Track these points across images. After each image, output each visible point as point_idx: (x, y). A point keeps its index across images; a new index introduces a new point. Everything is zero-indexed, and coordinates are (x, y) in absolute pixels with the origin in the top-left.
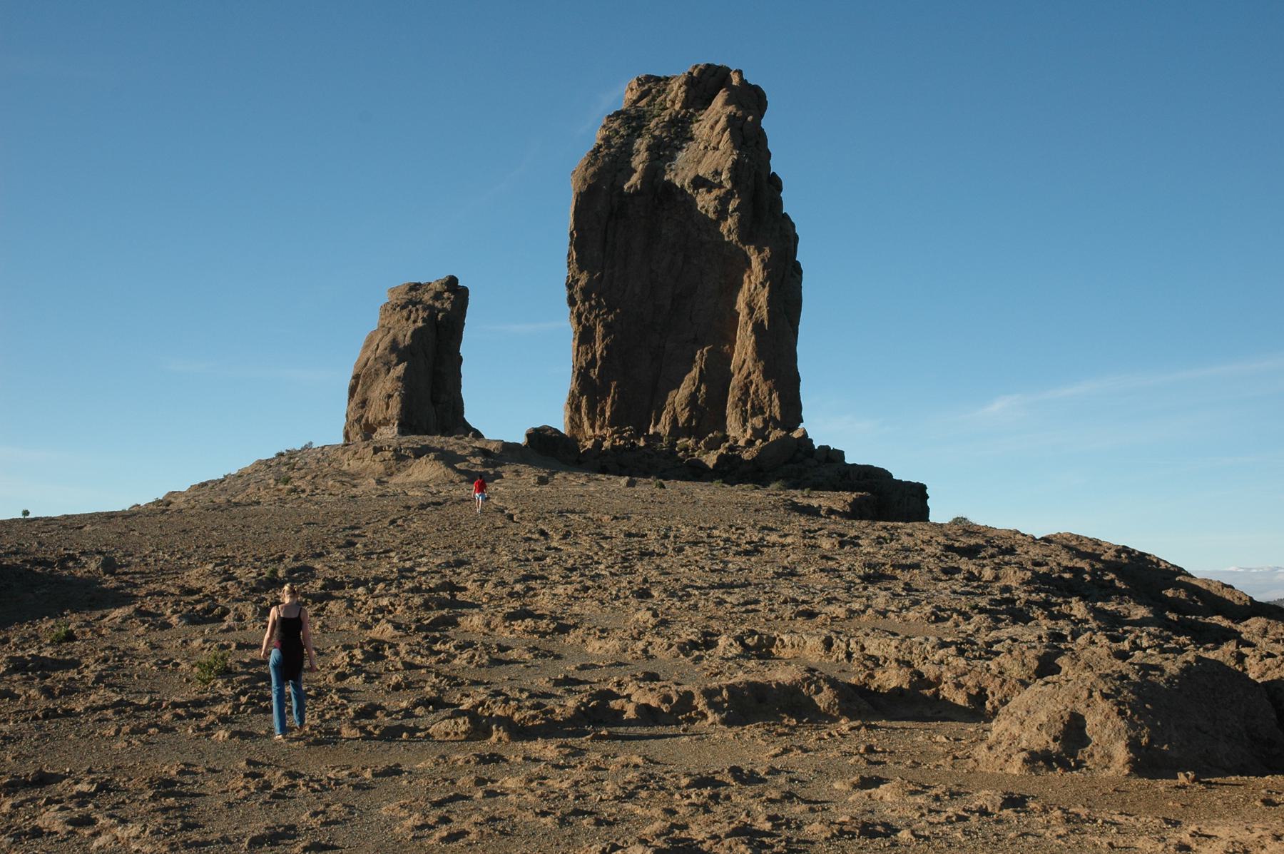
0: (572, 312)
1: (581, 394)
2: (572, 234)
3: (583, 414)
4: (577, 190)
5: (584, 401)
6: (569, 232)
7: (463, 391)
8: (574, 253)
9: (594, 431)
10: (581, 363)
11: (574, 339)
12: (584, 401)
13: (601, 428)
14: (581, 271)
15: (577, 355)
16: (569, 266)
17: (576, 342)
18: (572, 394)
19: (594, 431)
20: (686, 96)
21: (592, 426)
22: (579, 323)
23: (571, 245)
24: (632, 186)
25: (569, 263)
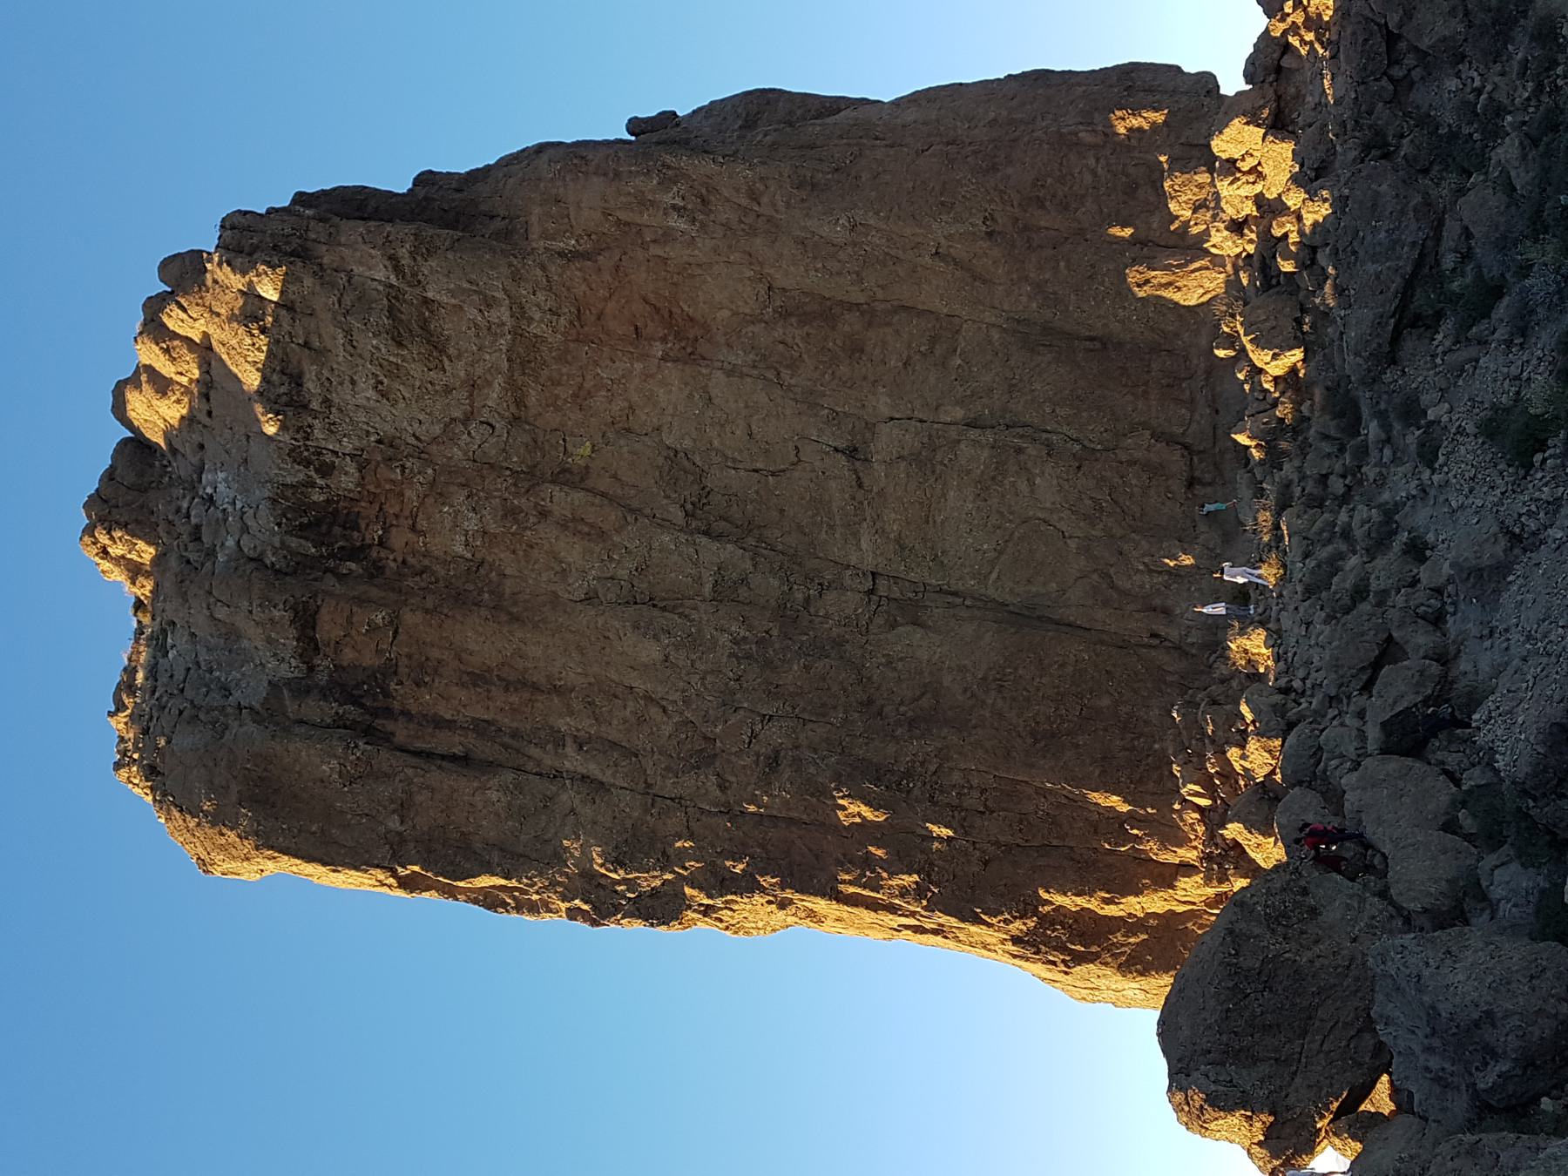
0: (707, 911)
1: (1028, 907)
2: (407, 884)
3: (1111, 911)
4: (248, 846)
5: (1059, 900)
6: (400, 893)
9: (1186, 869)
10: (904, 892)
11: (812, 915)
12: (1059, 900)
14: (557, 858)
15: (873, 906)
16: (533, 909)
17: (821, 905)
18: (1030, 945)
19: (1186, 869)
21: (1166, 877)
22: (748, 886)
23: (451, 893)
24: (269, 640)
25: (518, 909)
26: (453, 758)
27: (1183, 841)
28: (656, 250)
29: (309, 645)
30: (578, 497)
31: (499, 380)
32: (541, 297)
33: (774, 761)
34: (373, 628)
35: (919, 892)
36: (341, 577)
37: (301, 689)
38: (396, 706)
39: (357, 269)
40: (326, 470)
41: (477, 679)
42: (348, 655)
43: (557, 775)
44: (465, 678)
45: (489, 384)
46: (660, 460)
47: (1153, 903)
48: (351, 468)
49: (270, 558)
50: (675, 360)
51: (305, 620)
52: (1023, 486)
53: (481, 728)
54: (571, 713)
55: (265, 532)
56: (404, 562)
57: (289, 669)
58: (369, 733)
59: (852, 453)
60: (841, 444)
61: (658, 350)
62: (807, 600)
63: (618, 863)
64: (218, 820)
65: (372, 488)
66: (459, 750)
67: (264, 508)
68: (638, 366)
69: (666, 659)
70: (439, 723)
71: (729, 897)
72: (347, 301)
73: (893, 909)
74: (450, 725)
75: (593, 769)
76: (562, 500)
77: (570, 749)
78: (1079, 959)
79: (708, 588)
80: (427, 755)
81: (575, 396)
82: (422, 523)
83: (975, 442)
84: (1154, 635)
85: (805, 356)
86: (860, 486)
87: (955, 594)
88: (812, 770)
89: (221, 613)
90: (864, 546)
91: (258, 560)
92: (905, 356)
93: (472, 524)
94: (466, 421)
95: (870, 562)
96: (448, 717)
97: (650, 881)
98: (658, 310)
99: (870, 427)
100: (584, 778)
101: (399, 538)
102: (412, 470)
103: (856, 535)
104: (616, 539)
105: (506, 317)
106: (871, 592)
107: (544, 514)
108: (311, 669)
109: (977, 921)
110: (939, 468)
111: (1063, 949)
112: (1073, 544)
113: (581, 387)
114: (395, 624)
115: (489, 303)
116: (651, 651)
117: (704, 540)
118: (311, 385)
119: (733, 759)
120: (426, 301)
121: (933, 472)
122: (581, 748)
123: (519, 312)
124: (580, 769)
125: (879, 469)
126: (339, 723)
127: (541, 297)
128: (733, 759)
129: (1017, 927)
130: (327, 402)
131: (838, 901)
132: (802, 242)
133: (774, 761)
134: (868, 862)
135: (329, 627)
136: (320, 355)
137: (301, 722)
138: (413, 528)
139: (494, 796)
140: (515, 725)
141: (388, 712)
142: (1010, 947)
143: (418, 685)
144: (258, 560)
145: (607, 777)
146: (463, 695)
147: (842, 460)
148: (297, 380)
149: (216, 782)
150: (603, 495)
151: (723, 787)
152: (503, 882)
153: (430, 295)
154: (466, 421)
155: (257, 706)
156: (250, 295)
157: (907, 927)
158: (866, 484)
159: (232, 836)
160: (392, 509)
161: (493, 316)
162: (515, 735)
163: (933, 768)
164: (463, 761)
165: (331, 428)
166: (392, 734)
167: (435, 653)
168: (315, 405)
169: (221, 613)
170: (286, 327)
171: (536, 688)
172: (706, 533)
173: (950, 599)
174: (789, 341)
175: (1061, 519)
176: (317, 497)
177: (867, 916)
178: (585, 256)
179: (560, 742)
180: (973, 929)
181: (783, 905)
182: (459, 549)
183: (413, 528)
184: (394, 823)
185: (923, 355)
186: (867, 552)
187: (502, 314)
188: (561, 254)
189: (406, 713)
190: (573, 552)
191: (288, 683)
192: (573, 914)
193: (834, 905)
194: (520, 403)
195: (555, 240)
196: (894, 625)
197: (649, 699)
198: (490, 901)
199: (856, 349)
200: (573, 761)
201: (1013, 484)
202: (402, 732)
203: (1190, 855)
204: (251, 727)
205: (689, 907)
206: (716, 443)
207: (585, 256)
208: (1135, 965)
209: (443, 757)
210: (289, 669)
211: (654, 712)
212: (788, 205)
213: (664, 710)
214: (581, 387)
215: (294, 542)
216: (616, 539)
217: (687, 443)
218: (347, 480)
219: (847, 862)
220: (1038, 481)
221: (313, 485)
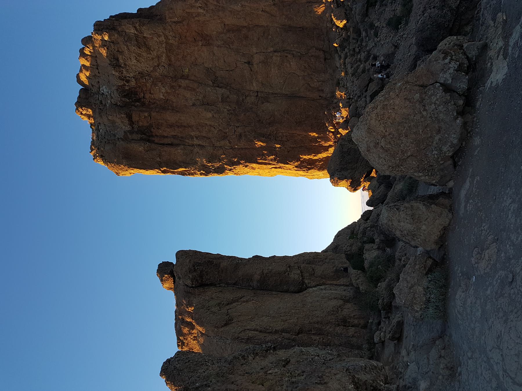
0: (230, 170)
1: (298, 159)
2: (164, 172)
3: (315, 158)
5: (305, 157)
6: (162, 174)
7: (291, 254)
8: (181, 170)
9: (330, 146)
10: (272, 160)
11: (253, 168)
12: (305, 157)
13: (327, 140)
14: (196, 163)
16: (192, 174)
17: (254, 165)
18: (299, 167)
20: (85, 106)
21: (326, 149)
22: (238, 163)
23: (173, 173)
24: (122, 122)
25: (189, 175)
26: (169, 144)
27: (329, 140)
28: (197, 19)
29: (131, 123)
30: (187, 81)
31: (164, 55)
32: (171, 33)
33: (240, 136)
34: (145, 117)
35: (275, 159)
36: (135, 106)
37: (131, 132)
38: (154, 134)
39: (127, 31)
40: (128, 81)
41: (171, 126)
42: (141, 124)
43: (193, 145)
44: (168, 126)
45: (162, 56)
46: (205, 71)
47: (324, 155)
48: (133, 80)
49: (119, 104)
50: (205, 46)
51: (129, 117)
52: (288, 65)
53: (174, 137)
54: (194, 131)
55: (116, 97)
56: (150, 101)
57: (128, 128)
58: (149, 141)
59: (249, 63)
60: (246, 61)
61: (200, 43)
62: (243, 99)
63: (210, 162)
64: (119, 163)
65: (139, 85)
66: (170, 142)
67: (115, 92)
68: (196, 48)
69: (213, 116)
70: (164, 137)
71: (234, 166)
72: (126, 39)
73: (270, 164)
74: (167, 137)
75: (200, 143)
76: (184, 83)
77: (195, 139)
78: (310, 169)
79: (220, 99)
80: (163, 144)
81: (183, 57)
82: (152, 92)
83: (277, 56)
84: (320, 96)
85: (235, 41)
86: (251, 70)
87: (276, 94)
88: (249, 137)
89: (110, 117)
90: (254, 85)
91: (116, 104)
92: (258, 37)
93: (163, 90)
94: (158, 66)
95: (256, 89)
96: (166, 135)
97: (217, 165)
98: (199, 34)
99: (252, 56)
100: (199, 145)
101: (147, 96)
102: (147, 79)
103: (252, 83)
104: (198, 90)
105: (163, 39)
106: (257, 96)
107: (180, 86)
108: (133, 128)
109: (288, 164)
110: (269, 63)
111: (306, 167)
112: (300, 78)
113: (184, 55)
114: (150, 115)
115: (159, 36)
116: (209, 115)
117: (218, 88)
118: (121, 61)
119: (231, 136)
120: (144, 37)
121: (268, 65)
122: (197, 138)
123: (166, 37)
124: (198, 143)
125: (255, 66)
126: (141, 139)
127: (171, 33)
128: (231, 136)
129: (296, 164)
130: (125, 64)
131: (258, 164)
132: (231, 12)
133: (240, 136)
134: (263, 155)
135: (135, 118)
136: (121, 53)
137: (133, 140)
138: (150, 93)
139: (179, 151)
140: (181, 135)
141: (152, 136)
142: (295, 169)
143: (158, 129)
144: (116, 104)
145: (204, 144)
146: (168, 130)
147: (247, 65)
148: (117, 60)
149: (116, 155)
150: (193, 80)
151: (230, 143)
152: (185, 169)
153: (145, 35)
154: (158, 66)
155: (122, 137)
156: (103, 40)
157: (273, 168)
158: (253, 69)
159: (122, 166)
160: (144, 89)
161: (160, 39)
162: (182, 138)
163: (275, 133)
164: (171, 145)
165: (127, 71)
166: (154, 140)
167: (161, 121)
168: (122, 65)
169: (110, 117)
170: (113, 47)
171: (185, 127)
172: (218, 87)
173: (275, 95)
174: (230, 37)
175: (297, 72)
176: (127, 88)
177: (264, 166)
178: (180, 22)
179: (192, 138)
180: (287, 166)
181: (246, 166)
182: (162, 97)
183: (150, 93)
184: (158, 159)
185: (262, 36)
186: (255, 87)
187: (163, 38)
188: (174, 22)
189: (156, 136)
190: (188, 94)
191: (128, 131)
192: (201, 174)
193: (257, 165)
194: (170, 60)
195: (172, 19)
196: (263, 103)
197: (211, 126)
198: (183, 174)
199: (246, 37)
200: (196, 142)
201: (286, 65)
202: (156, 140)
203: (331, 143)
204: (122, 142)
205: (226, 170)
206: (217, 65)
207: (180, 22)
208: (321, 169)
209: (167, 144)
210: (128, 128)
211: (212, 128)
212: (226, 3)
213: (215, 128)
214: (184, 55)
215: (123, 99)
216: (198, 90)
217: (210, 65)
218: (133, 83)
219: (259, 155)
220: (291, 63)
221: (125, 85)
